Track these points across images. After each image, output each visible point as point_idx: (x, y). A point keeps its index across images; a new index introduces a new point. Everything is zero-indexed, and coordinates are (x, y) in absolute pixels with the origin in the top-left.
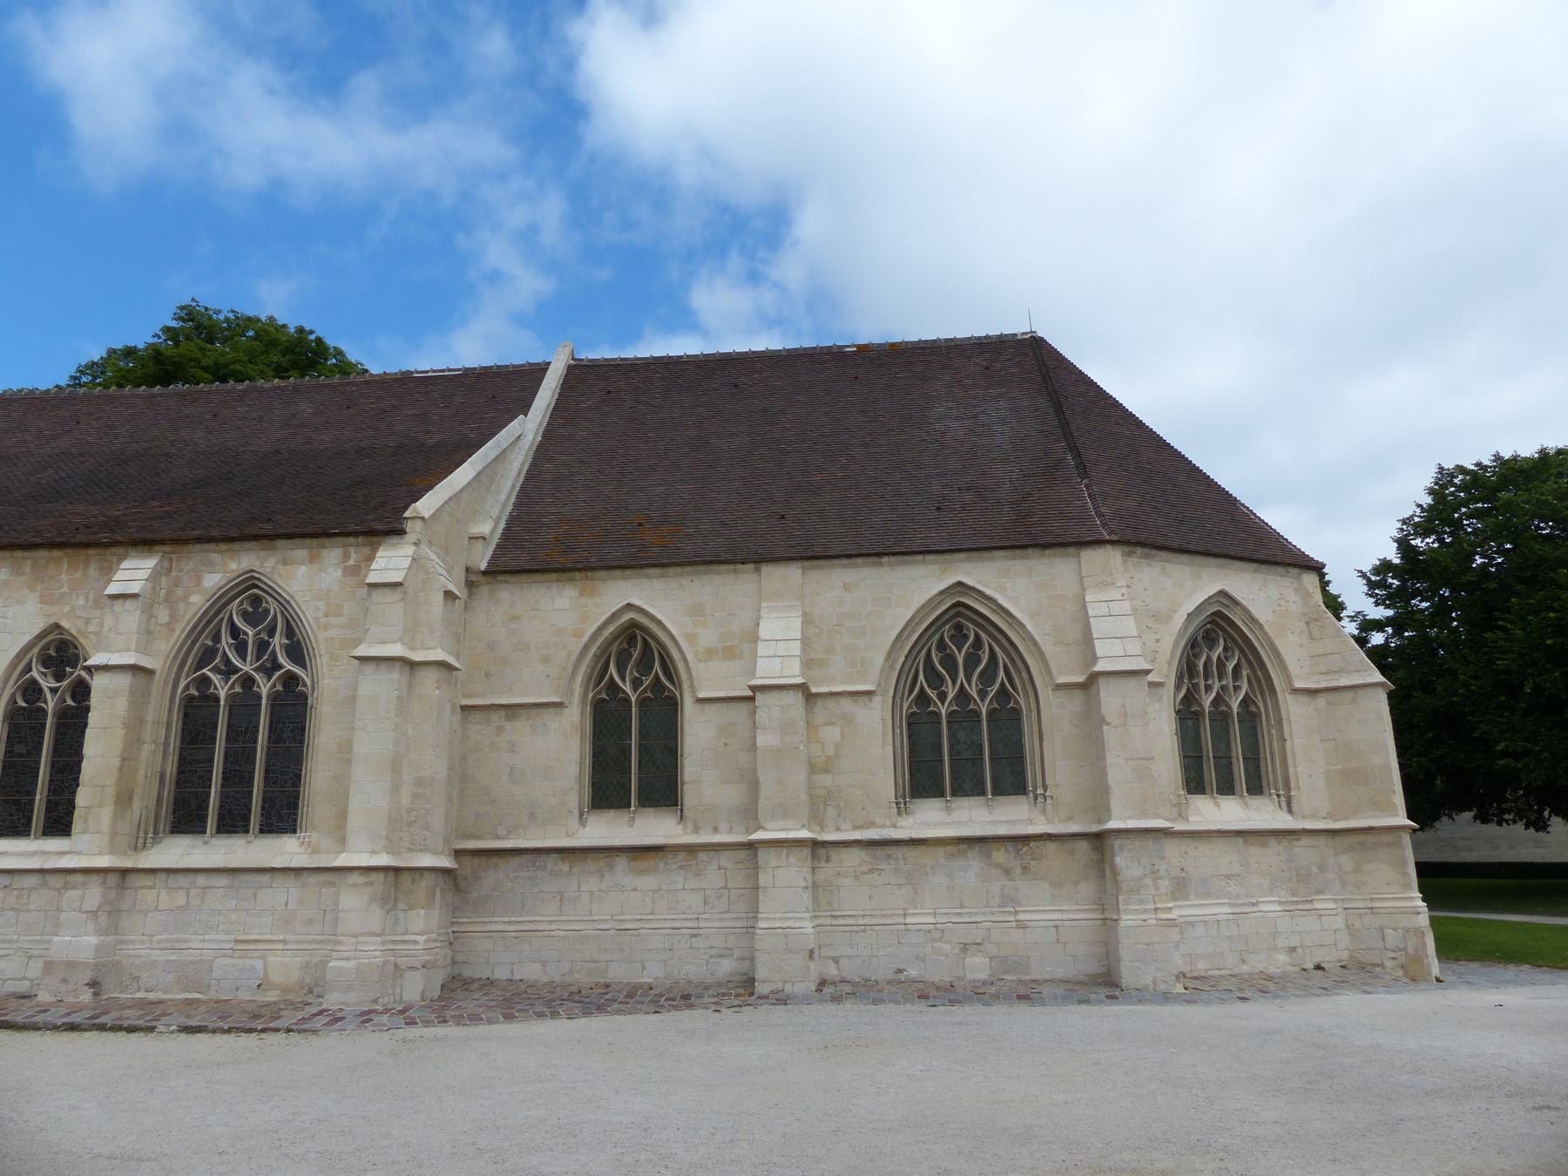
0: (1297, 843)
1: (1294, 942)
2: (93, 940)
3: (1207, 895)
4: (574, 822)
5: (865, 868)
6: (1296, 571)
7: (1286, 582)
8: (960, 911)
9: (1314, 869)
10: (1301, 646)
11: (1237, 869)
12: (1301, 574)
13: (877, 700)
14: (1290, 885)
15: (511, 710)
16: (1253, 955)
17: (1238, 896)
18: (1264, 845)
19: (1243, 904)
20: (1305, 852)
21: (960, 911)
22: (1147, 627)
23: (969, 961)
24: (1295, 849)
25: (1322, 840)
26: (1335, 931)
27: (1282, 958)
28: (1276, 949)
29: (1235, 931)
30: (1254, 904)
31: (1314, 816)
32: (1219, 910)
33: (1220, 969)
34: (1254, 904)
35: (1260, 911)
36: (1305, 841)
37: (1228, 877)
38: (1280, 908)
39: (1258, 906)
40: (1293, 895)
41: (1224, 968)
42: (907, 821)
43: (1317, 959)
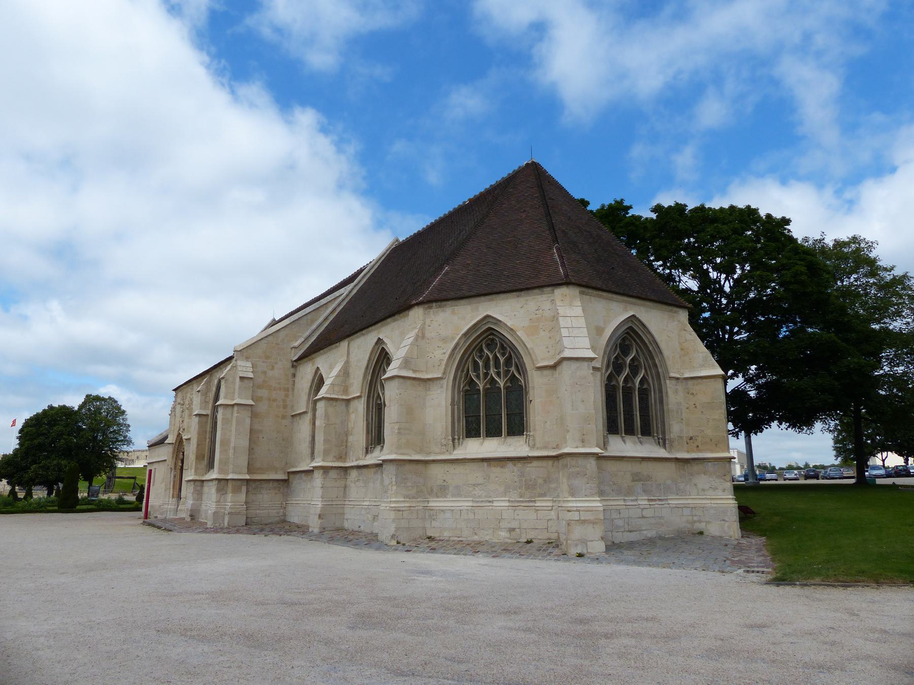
0: (529, 465)
1: (514, 525)
2: (191, 502)
3: (459, 495)
4: (308, 460)
5: (356, 479)
6: (549, 289)
7: (545, 297)
8: (375, 500)
9: (540, 481)
10: (550, 338)
11: (481, 480)
12: (553, 290)
13: (363, 399)
14: (519, 491)
15: (300, 414)
16: (482, 531)
17: (479, 497)
18: (502, 467)
19: (482, 501)
20: (532, 470)
21: (375, 500)
22: (438, 347)
23: (375, 523)
24: (528, 469)
25: (550, 462)
26: (548, 520)
27: (504, 534)
28: (500, 528)
29: (471, 516)
30: (490, 502)
31: (545, 448)
32: (465, 504)
33: (459, 537)
34: (490, 502)
35: (492, 506)
36: (535, 463)
37: (474, 485)
38: (507, 504)
39: (493, 503)
40: (521, 497)
41: (461, 537)
42: (369, 456)
43: (529, 537)
